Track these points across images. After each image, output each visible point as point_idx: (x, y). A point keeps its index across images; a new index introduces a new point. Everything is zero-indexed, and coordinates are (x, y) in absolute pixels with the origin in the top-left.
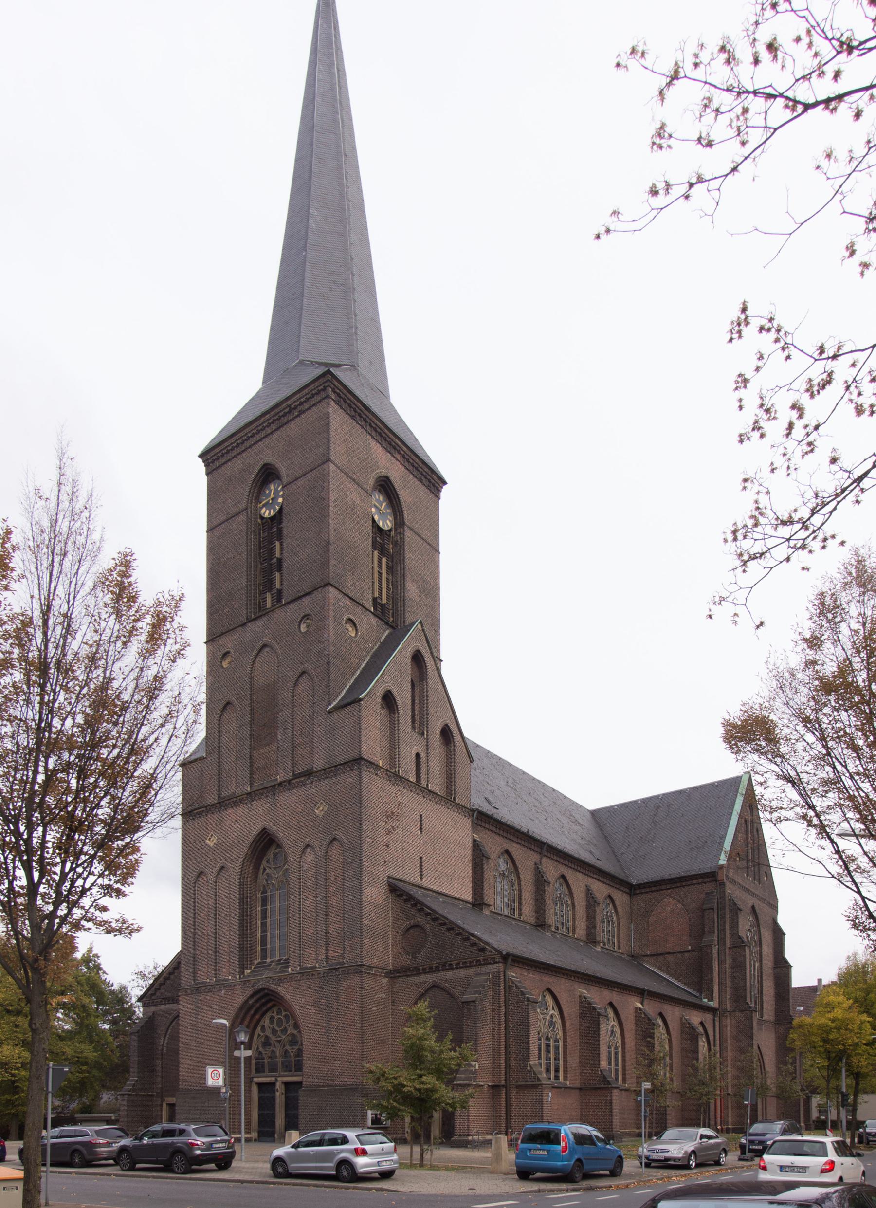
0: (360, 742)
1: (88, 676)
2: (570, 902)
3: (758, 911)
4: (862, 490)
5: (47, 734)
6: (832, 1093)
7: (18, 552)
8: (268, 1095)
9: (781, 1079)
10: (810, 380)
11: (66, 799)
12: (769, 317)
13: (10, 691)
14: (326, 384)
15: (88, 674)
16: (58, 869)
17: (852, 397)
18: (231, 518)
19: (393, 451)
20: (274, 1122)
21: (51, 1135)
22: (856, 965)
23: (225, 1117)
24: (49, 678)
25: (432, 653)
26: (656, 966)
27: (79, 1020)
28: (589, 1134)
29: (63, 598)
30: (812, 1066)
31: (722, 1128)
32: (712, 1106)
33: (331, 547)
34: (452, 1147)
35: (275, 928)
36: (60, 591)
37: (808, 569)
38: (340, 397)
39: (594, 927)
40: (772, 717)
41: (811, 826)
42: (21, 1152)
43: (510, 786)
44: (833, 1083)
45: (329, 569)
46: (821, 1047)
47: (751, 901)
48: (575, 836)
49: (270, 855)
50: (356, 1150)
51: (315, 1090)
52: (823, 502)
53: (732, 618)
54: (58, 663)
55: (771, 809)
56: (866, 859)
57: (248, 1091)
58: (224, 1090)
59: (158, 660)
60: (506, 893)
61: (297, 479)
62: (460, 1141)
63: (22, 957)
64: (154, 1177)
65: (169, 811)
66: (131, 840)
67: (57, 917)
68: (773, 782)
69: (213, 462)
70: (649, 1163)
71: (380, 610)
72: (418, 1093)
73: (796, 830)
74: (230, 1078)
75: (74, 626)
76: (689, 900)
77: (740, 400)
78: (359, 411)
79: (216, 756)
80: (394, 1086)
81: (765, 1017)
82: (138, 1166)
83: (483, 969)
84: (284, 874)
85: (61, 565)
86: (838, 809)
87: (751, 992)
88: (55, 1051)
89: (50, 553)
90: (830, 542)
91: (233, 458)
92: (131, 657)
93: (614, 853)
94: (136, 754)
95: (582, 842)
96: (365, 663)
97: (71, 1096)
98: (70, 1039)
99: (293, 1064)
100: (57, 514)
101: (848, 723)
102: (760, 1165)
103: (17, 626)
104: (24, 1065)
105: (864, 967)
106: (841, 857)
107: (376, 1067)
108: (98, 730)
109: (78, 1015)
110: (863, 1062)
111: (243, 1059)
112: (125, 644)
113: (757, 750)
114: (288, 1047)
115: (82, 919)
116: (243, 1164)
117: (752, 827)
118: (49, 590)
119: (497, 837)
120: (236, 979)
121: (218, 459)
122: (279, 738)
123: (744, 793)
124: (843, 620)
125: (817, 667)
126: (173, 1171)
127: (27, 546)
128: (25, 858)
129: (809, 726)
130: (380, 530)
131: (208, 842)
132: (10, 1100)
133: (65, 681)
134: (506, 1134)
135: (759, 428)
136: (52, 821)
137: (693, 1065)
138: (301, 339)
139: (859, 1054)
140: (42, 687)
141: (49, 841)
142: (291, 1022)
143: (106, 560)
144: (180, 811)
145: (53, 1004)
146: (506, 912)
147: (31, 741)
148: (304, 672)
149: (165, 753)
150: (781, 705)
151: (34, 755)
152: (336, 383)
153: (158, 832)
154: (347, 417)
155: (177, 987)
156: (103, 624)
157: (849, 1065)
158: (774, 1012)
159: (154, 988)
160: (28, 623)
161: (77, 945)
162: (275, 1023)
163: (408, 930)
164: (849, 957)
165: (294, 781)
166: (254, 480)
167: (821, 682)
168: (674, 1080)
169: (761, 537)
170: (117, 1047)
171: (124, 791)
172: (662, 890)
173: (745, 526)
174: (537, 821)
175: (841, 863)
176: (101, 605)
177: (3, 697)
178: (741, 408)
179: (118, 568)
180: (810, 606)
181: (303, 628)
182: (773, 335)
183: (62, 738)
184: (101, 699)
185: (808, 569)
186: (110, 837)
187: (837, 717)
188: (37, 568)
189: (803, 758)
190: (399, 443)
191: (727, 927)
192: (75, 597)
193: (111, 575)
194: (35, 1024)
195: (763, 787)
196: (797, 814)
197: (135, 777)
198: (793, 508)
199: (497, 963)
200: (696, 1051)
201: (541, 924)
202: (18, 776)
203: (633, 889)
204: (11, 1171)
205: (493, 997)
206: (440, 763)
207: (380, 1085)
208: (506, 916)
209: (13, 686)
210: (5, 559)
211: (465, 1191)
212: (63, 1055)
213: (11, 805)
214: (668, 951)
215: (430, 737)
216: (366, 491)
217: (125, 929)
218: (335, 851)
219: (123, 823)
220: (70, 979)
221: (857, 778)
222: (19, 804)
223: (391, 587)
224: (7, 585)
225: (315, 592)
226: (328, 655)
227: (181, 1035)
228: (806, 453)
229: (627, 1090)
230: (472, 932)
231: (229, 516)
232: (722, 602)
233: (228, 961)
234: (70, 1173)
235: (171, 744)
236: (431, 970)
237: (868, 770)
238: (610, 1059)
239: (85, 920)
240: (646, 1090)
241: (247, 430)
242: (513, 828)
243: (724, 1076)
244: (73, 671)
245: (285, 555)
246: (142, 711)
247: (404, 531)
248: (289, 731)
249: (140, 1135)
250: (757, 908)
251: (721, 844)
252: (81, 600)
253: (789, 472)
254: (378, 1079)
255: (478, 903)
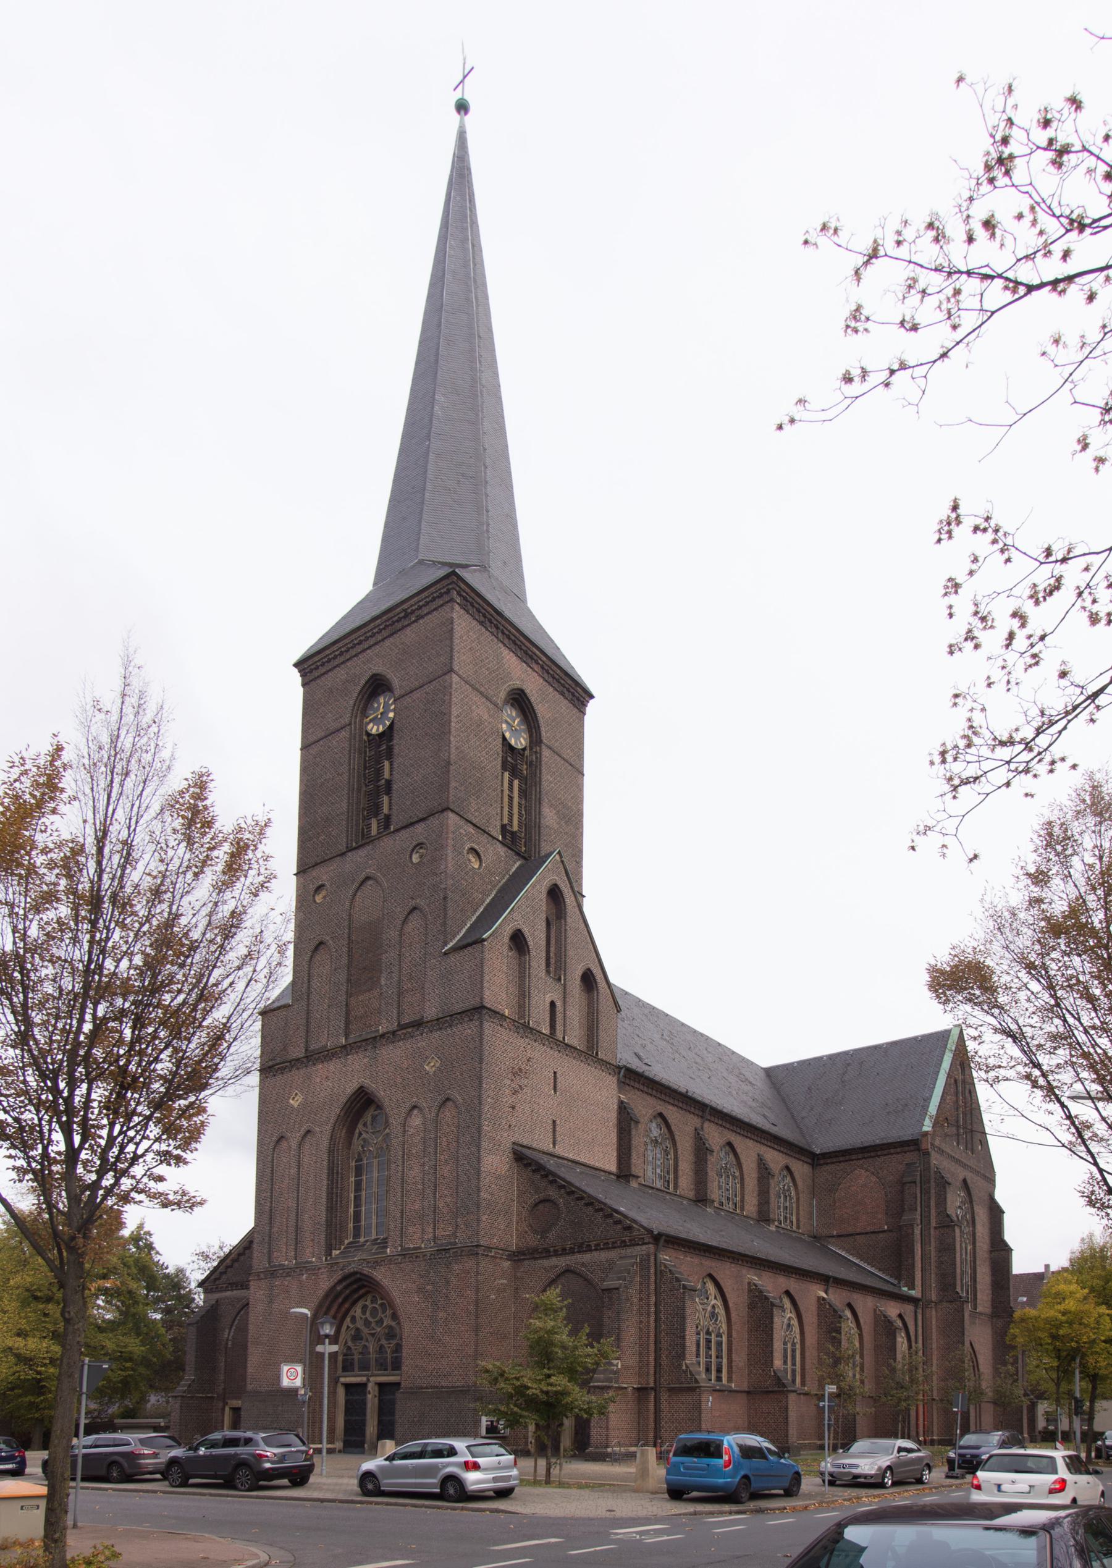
0: (482, 988)
1: (150, 911)
2: (737, 1174)
3: (970, 1185)
4: (1098, 708)
5: (97, 977)
6: (1063, 1398)
7: (69, 771)
8: (358, 1397)
9: (999, 1382)
10: (1035, 585)
11: (118, 1051)
12: (985, 516)
13: (54, 928)
14: (450, 587)
15: (150, 909)
16: (104, 1133)
17: (1085, 605)
18: (330, 734)
19: (529, 661)
20: (364, 1430)
21: (83, 1444)
22: (1092, 1248)
23: (303, 1424)
24: (102, 914)
25: (572, 888)
26: (843, 1249)
27: (124, 1309)
28: (758, 1445)
29: (122, 823)
30: (1037, 1366)
31: (925, 1440)
32: (913, 1413)
33: (452, 768)
34: (586, 1460)
35: (371, 1202)
36: (120, 815)
37: (1032, 796)
38: (467, 601)
39: (768, 1202)
40: (989, 962)
41: (1037, 1087)
42: (45, 1465)
43: (665, 1040)
44: (1064, 1387)
45: (448, 792)
46: (1048, 1344)
47: (962, 1173)
48: (745, 1098)
49: (368, 1117)
50: (466, 1463)
51: (416, 1392)
52: (1050, 721)
53: (940, 850)
54: (114, 898)
55: (987, 1067)
56: (1104, 1126)
57: (333, 1393)
58: (302, 1392)
59: (236, 894)
60: (658, 1163)
61: (411, 692)
62: (597, 1453)
63: (56, 1234)
64: (211, 1495)
65: (244, 1066)
66: (197, 1100)
67: (101, 1188)
68: (989, 1036)
69: (311, 672)
70: (833, 1481)
71: (510, 839)
72: (545, 1396)
73: (1018, 1092)
74: (311, 1377)
75: (135, 855)
76: (885, 1172)
77: (950, 607)
78: (489, 616)
79: (304, 1003)
80: (515, 1388)
81: (980, 1309)
82: (191, 1481)
83: (628, 1251)
84: (384, 1140)
85: (122, 785)
86: (1069, 1068)
87: (962, 1280)
88: (92, 1344)
89: (108, 772)
90: (1059, 765)
91: (335, 667)
92: (203, 890)
93: (793, 1117)
94: (206, 1001)
95: (754, 1104)
96: (490, 898)
97: (111, 1398)
98: (112, 1331)
99: (389, 1361)
100: (119, 729)
101: (1081, 970)
102: (972, 1483)
103: (65, 854)
104: (52, 1361)
105: (1102, 1250)
106: (1073, 1123)
107: (494, 1365)
108: (160, 972)
109: (123, 1303)
110: (1101, 1362)
111: (327, 1356)
112: (196, 875)
113: (970, 1000)
114: (383, 1342)
115: (132, 1190)
116: (324, 1480)
117: (964, 1088)
118: (106, 814)
119: (648, 1098)
120: (322, 1262)
121: (317, 668)
122: (383, 983)
123: (953, 1048)
124: (1075, 853)
125: (1043, 906)
126: (235, 1488)
127: (81, 764)
128: (64, 1119)
129: (1034, 972)
130: (512, 748)
131: (291, 1101)
132: (34, 1402)
133: (122, 917)
134: (655, 1445)
135: (973, 638)
136: (99, 1076)
137: (889, 1365)
138: (422, 536)
139: (1097, 1353)
140: (94, 923)
141: (95, 1100)
142: (389, 1312)
143: (177, 781)
144: (257, 1065)
145: (93, 1289)
146: (659, 1184)
147: (77, 985)
148: (415, 908)
149: (241, 999)
150: (1000, 949)
151: (80, 1000)
152: (462, 586)
153: (230, 1089)
154: (475, 622)
155: (248, 1271)
156: (171, 853)
157: (1084, 1367)
158: (989, 1303)
159: (218, 1272)
160: (78, 850)
161: (124, 1220)
162: (368, 1313)
163: (536, 1205)
164: (1083, 1239)
165: (400, 1033)
166: (360, 693)
167: (1049, 923)
168: (866, 1381)
169: (976, 759)
170: (170, 1340)
171: (190, 1042)
172: (852, 1160)
173: (956, 746)
174: (698, 1080)
175: (1073, 1130)
176: (169, 831)
177: (45, 935)
178: (951, 615)
179: (192, 789)
180: (1035, 837)
181: (415, 858)
182: (990, 535)
183: (115, 981)
184: (166, 937)
185: (1032, 796)
186: (170, 1095)
187: (1068, 963)
188: (92, 789)
189: (1027, 1010)
190: (537, 652)
191: (933, 1203)
192: (137, 822)
193: (182, 797)
194: (69, 1312)
195: (977, 1042)
196: (1019, 1073)
197: (203, 1027)
198: (1014, 727)
199: (646, 1244)
200: (893, 1348)
201: (701, 1199)
202: (60, 1025)
203: (815, 1160)
204: (32, 1486)
205: (641, 1284)
206: (579, 1012)
207: (498, 1386)
208: (658, 1189)
209: (58, 922)
210: (54, 779)
211: (601, 1512)
212: (102, 1349)
213: (49, 1058)
214: (858, 1231)
215: (569, 984)
216: (496, 705)
217: (185, 1202)
218: (448, 1114)
219: (187, 1080)
220: (115, 1260)
221: (1092, 1032)
222: (60, 1057)
223: (523, 812)
224: (55, 808)
225: (431, 818)
226: (445, 888)
227: (251, 1327)
228: (1030, 666)
229: (806, 1394)
230: (616, 1207)
231: (328, 732)
232: (928, 832)
233: (313, 1240)
234: (106, 1489)
235: (249, 989)
236: (564, 1252)
237: (1106, 1023)
238: (785, 1357)
239: (136, 1192)
240: (830, 1394)
241: (353, 637)
242: (668, 1088)
243: (928, 1378)
244: (132, 906)
245: (396, 776)
246: (215, 951)
247: (540, 750)
248: (395, 977)
249: (195, 1445)
250: (969, 1181)
251: (925, 1108)
252: (145, 825)
253: (1010, 686)
254: (496, 1379)
255: (624, 1174)
